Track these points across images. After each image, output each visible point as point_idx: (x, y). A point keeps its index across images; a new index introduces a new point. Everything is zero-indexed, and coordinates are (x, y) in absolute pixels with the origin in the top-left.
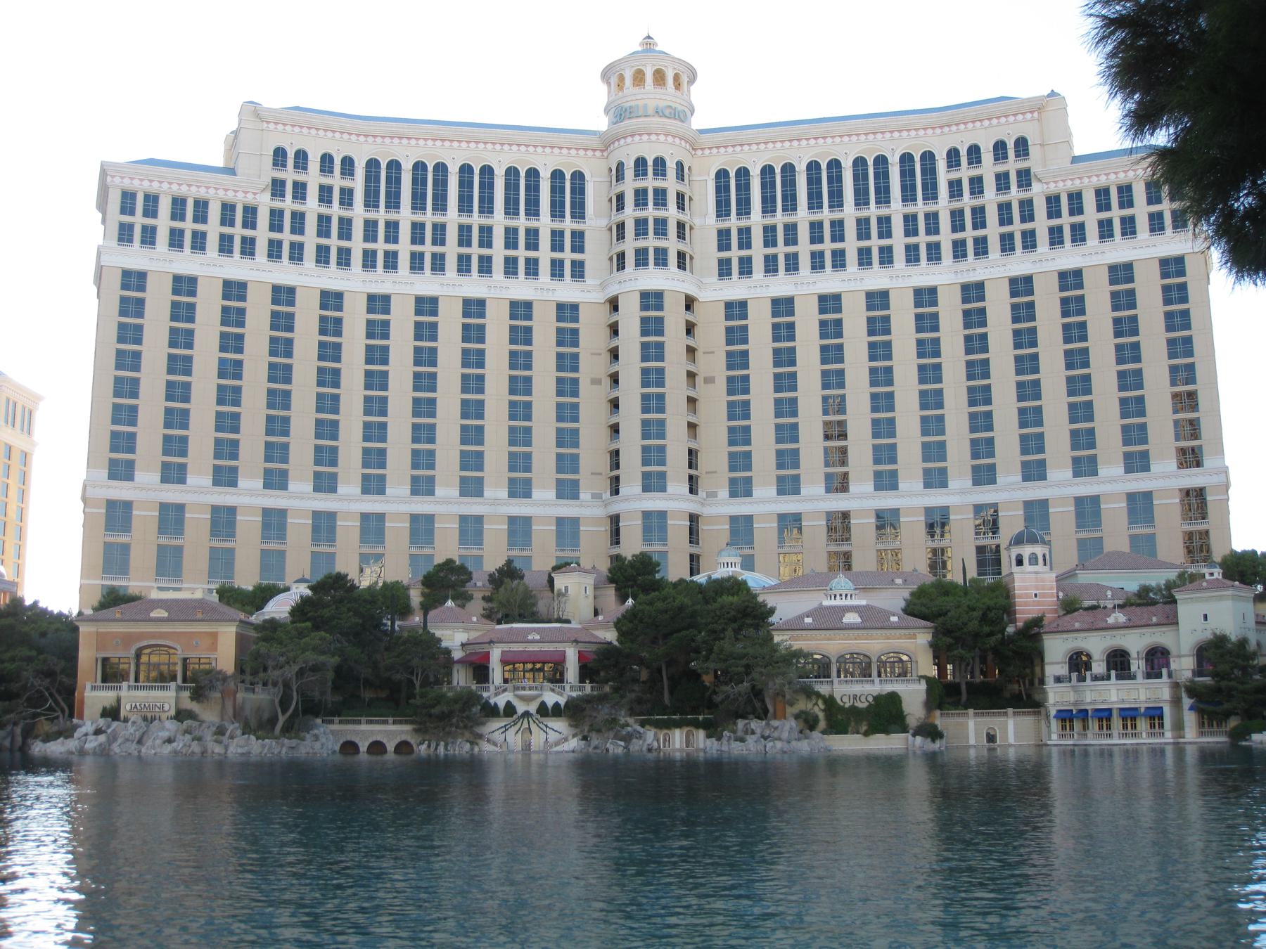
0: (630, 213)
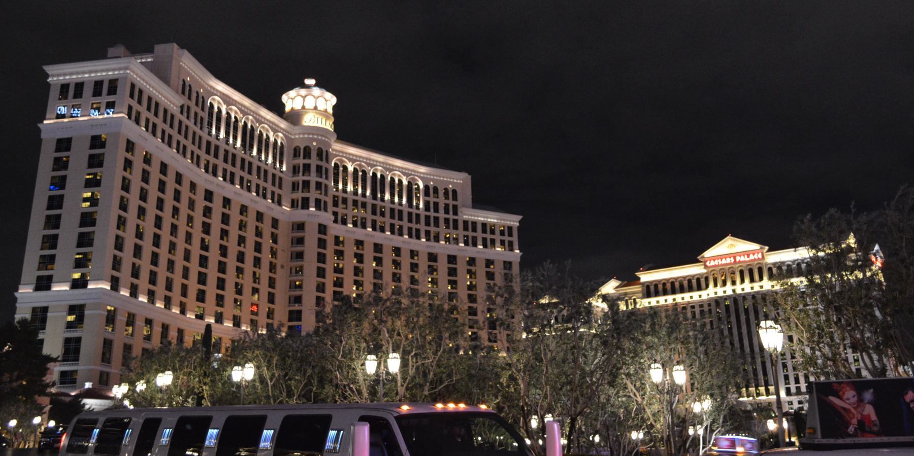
0: (313, 178)
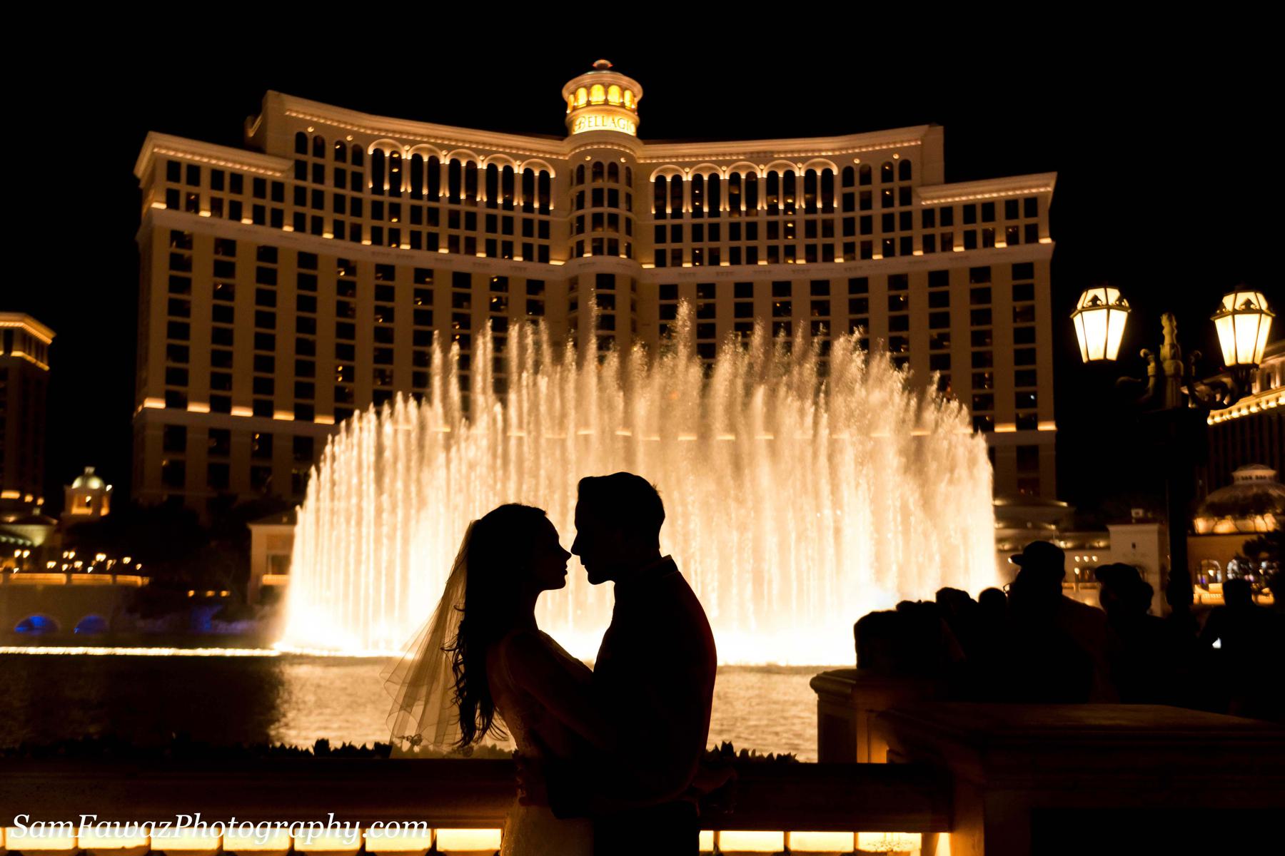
0: (589, 210)
